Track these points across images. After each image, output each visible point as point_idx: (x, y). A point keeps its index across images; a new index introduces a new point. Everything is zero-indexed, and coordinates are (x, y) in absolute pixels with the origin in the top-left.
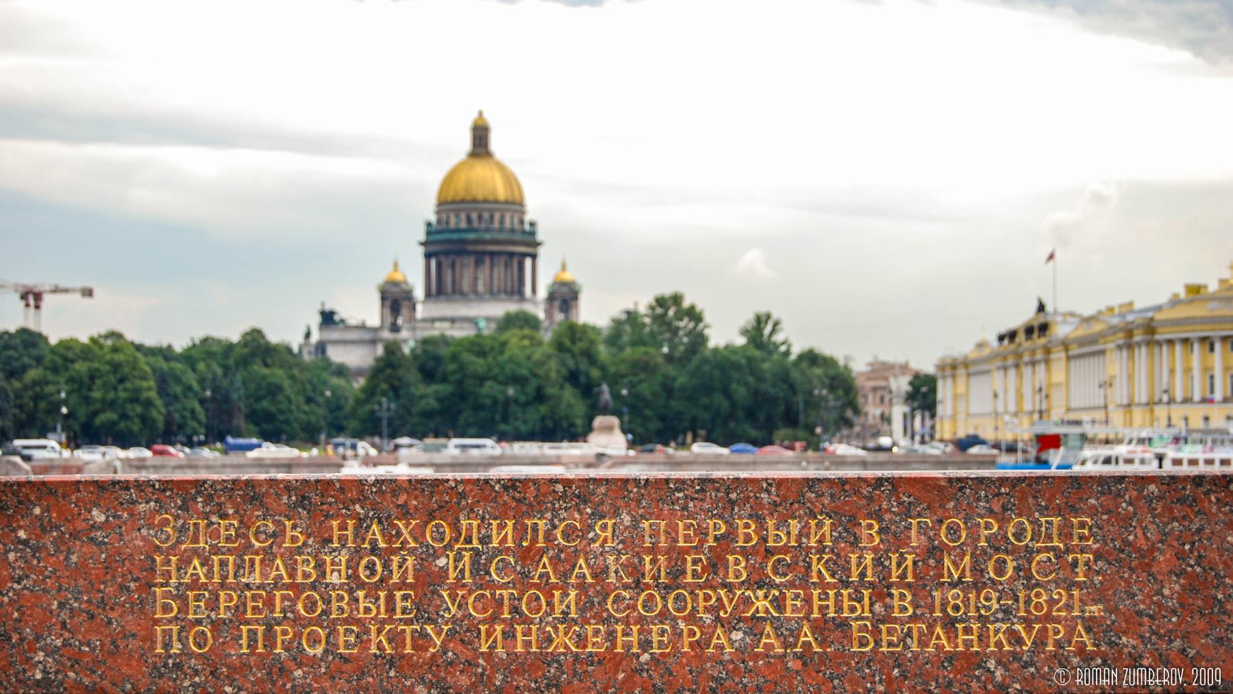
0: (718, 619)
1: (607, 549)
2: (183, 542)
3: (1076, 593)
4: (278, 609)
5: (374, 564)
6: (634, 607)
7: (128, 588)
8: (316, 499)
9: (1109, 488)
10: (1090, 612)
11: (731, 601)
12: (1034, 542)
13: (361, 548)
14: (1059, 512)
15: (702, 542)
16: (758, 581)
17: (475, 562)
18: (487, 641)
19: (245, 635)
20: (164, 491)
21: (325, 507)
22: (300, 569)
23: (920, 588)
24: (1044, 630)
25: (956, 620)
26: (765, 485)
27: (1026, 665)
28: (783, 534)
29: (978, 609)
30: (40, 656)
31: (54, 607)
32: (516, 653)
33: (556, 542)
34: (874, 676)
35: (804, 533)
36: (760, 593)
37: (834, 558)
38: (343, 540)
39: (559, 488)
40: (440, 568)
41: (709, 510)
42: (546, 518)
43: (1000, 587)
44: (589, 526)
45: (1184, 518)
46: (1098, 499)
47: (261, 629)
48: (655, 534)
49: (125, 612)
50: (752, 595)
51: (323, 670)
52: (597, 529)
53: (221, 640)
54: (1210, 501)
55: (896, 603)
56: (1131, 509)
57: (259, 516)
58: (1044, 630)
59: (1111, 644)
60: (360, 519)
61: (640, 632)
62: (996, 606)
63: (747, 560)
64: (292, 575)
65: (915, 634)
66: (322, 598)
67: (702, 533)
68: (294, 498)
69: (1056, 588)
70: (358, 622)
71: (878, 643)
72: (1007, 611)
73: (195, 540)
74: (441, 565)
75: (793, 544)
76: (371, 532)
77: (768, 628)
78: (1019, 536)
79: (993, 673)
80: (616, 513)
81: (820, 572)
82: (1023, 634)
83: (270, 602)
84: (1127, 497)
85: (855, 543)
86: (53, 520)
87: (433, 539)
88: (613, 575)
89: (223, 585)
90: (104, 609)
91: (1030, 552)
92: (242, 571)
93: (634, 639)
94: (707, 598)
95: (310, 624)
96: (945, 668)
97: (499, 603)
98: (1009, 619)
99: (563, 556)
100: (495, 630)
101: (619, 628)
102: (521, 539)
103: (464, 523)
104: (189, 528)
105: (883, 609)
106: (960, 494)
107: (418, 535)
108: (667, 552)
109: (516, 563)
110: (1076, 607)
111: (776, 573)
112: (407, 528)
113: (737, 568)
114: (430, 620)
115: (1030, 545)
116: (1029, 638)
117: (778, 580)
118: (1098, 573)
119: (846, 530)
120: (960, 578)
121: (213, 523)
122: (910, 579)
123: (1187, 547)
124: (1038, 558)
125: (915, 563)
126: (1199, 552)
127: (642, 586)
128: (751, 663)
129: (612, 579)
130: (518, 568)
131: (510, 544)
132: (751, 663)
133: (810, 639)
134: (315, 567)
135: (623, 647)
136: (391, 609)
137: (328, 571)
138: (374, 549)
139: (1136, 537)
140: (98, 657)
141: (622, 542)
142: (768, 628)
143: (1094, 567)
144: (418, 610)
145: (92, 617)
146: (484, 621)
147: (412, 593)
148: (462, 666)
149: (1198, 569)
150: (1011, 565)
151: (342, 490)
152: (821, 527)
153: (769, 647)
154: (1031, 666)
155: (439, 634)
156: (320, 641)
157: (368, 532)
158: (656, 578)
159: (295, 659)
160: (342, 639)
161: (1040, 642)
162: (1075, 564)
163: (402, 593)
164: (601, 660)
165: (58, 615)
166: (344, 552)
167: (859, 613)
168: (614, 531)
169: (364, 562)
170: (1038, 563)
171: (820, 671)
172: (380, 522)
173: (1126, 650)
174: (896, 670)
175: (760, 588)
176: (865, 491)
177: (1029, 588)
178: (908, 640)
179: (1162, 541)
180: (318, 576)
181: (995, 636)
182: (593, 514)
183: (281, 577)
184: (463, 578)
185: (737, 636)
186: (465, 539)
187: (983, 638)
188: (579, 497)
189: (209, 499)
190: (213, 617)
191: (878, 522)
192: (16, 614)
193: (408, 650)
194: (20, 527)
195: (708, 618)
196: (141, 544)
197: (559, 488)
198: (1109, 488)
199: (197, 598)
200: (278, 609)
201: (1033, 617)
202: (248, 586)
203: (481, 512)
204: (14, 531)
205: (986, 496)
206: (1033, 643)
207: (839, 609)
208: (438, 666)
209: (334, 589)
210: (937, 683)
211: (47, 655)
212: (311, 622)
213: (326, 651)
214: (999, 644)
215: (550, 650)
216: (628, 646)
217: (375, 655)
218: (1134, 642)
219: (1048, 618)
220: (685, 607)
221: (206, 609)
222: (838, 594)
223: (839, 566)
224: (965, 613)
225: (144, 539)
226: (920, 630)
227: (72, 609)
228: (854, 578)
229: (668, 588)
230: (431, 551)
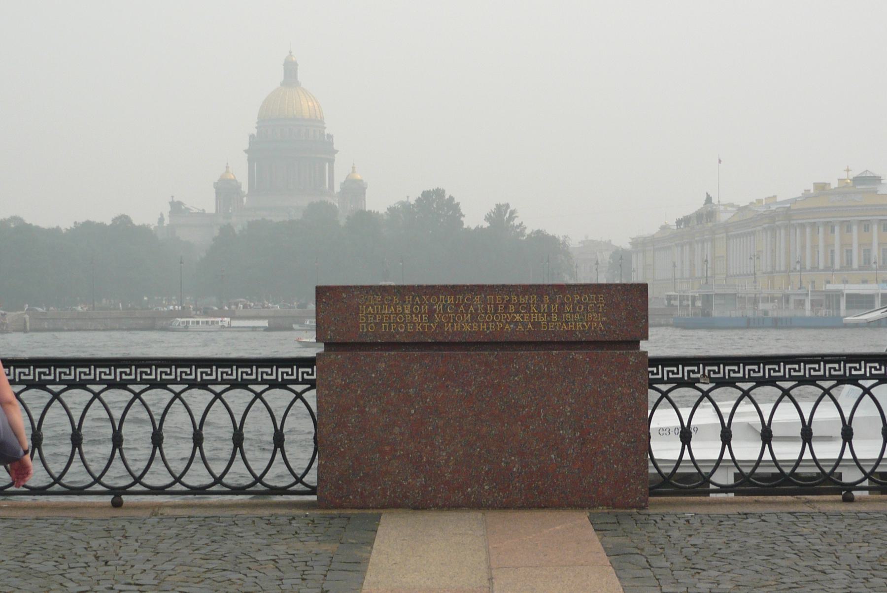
8: (402, 291)
14: (595, 293)
16: (517, 312)
22: (398, 309)
27: (586, 333)
28: (523, 300)
30: (329, 332)
35: (529, 299)
36: (518, 315)
38: (409, 301)
47: (388, 325)
48: (490, 298)
55: (553, 317)
64: (396, 310)
70: (413, 323)
71: (548, 328)
72: (581, 319)
73: (370, 302)
78: (585, 300)
80: (480, 294)
83: (390, 318)
85: (542, 302)
89: (377, 314)
93: (485, 327)
94: (504, 316)
97: (450, 318)
101: (481, 324)
103: (441, 297)
108: (494, 304)
111: (522, 309)
113: (512, 308)
114: (432, 322)
122: (557, 311)
129: (479, 311)
131: (453, 302)
133: (531, 327)
136: (422, 319)
138: (417, 304)
150: (583, 308)
151: (409, 289)
153: (520, 329)
158: (491, 311)
160: (409, 327)
161: (590, 327)
164: (476, 332)
167: (543, 320)
172: (419, 297)
176: (545, 288)
185: (512, 326)
187: (575, 326)
193: (426, 330)
195: (504, 321)
197: (466, 288)
199: (371, 317)
202: (384, 313)
207: (538, 319)
212: (401, 323)
213: (405, 330)
214: (580, 328)
216: (483, 329)
219: (592, 321)
222: (538, 315)
228: (542, 311)
229: (494, 314)
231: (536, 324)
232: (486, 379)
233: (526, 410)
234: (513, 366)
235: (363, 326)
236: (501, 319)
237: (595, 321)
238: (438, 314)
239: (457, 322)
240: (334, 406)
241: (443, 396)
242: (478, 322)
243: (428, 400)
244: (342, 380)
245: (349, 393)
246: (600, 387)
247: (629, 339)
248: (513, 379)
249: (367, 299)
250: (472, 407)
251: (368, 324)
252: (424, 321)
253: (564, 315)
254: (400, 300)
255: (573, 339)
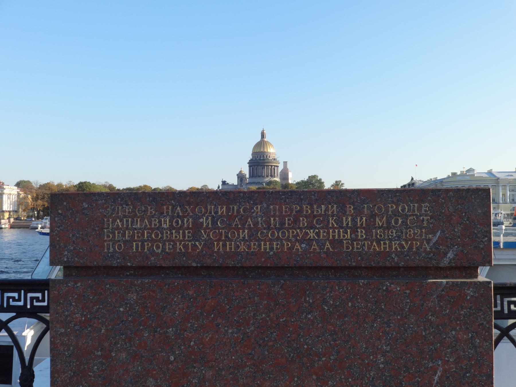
0: (297, 240)
1: (258, 216)
2: (113, 214)
3: (424, 230)
4: (146, 237)
5: (178, 221)
6: (268, 236)
7: (95, 230)
9: (435, 193)
10: (429, 237)
11: (301, 233)
12: (409, 213)
13: (174, 216)
15: (291, 213)
16: (311, 227)
17: (212, 220)
18: (217, 248)
19: (134, 246)
20: (107, 196)
21: (161, 202)
23: (368, 229)
24: (412, 244)
25: (381, 240)
26: (313, 193)
27: (406, 256)
29: (388, 236)
30: (66, 253)
31: (71, 236)
32: (227, 252)
33: (241, 213)
34: (352, 260)
35: (327, 210)
36: (312, 231)
37: (338, 218)
38: (167, 213)
39: (242, 194)
40: (201, 222)
41: (293, 202)
42: (237, 205)
43: (396, 229)
44: (252, 208)
45: (463, 204)
46: (431, 197)
48: (275, 210)
49: (94, 238)
50: (309, 232)
51: (161, 258)
52: (255, 208)
53: (126, 247)
54: (472, 198)
55: (359, 234)
56: (443, 201)
57: (139, 205)
58: (412, 244)
59: (436, 248)
60: (173, 206)
61: (270, 244)
62: (395, 235)
63: (307, 219)
64: (150, 224)
65: (366, 246)
66: (160, 233)
67: (291, 210)
68: (151, 199)
69: (417, 229)
70: (173, 241)
71: (353, 248)
73: (118, 213)
74: (201, 221)
75: (323, 213)
76: (177, 210)
77: (314, 243)
78: (403, 210)
79: (394, 258)
80: (261, 203)
81: (332, 223)
82: (405, 245)
83: (143, 234)
84: (442, 196)
85: (345, 214)
86: (70, 207)
87: (199, 212)
88: (260, 224)
89: (127, 228)
90: (87, 237)
91: (407, 216)
92: (133, 223)
93: (268, 246)
94: (293, 232)
95: (156, 242)
96: (377, 257)
98: (400, 240)
99: (243, 218)
100: (220, 244)
102: (229, 212)
104: (116, 209)
105: (355, 236)
106: (382, 196)
107: (193, 211)
109: (227, 220)
110: (424, 235)
112: (189, 209)
113: (303, 222)
114: (197, 240)
115: (407, 214)
116: (407, 247)
117: (318, 226)
118: (431, 223)
119: (342, 209)
120: (382, 225)
121: (124, 207)
123: (464, 214)
124: (410, 218)
125: (366, 220)
126: (468, 216)
127: (270, 228)
128: (308, 255)
129: (260, 226)
130: (228, 222)
132: (308, 255)
134: (158, 222)
135: (264, 249)
136: (184, 236)
137: (163, 223)
138: (178, 216)
139: (445, 211)
140: (85, 253)
141: (263, 213)
142: (314, 243)
143: (430, 221)
144: (193, 237)
145: (83, 240)
146: (215, 241)
147: (191, 231)
148: (208, 256)
149: (468, 222)
150: (400, 221)
151: (167, 196)
152: (333, 208)
154: (408, 256)
155: (200, 245)
156: (160, 248)
157: (176, 210)
158: (275, 225)
159: (151, 254)
161: (411, 247)
162: (423, 220)
163: (188, 231)
165: (72, 239)
166: (168, 217)
168: (261, 209)
169: (174, 221)
170: (410, 220)
171: (333, 258)
172: (180, 207)
173: (442, 251)
174: (360, 258)
175: (312, 229)
177: (407, 229)
178: (364, 247)
179: (454, 212)
180: (159, 225)
181: (395, 246)
182: (253, 203)
183: (147, 225)
184: (209, 226)
185: (303, 246)
186: (209, 212)
188: (248, 197)
189: (122, 199)
190: (124, 239)
191: (353, 206)
192: (58, 239)
193: (190, 250)
194: (59, 209)
196: (100, 214)
197: (242, 194)
198: (435, 193)
200: (146, 237)
201: (408, 239)
202: (135, 229)
203: (215, 203)
204: (57, 210)
205: (391, 197)
206: (408, 248)
208: (200, 256)
209: (165, 230)
210: (374, 262)
211: (68, 253)
212: (156, 241)
213: (162, 251)
214: (396, 248)
215: (238, 250)
217: (178, 252)
218: (445, 248)
219: (413, 239)
220: (285, 235)
221: (121, 237)
222: (339, 231)
223: (339, 221)
224: (384, 238)
225: (100, 213)
226: (368, 243)
227: (77, 237)
228: (345, 225)
229: (279, 229)
230: (198, 217)
231: (337, 243)
232: (269, 316)
233: (324, 359)
234: (305, 299)
235: (108, 245)
236: (289, 236)
237: (417, 240)
238: (205, 230)
239: (230, 240)
240: (71, 348)
241: (211, 338)
242: (259, 240)
243: (192, 343)
244: (82, 315)
245: (90, 331)
246: (425, 330)
247: (466, 264)
248: (306, 317)
249: (114, 210)
250: (250, 354)
251: (115, 242)
252: (187, 238)
253: (374, 231)
254: (156, 212)
255: (388, 264)
